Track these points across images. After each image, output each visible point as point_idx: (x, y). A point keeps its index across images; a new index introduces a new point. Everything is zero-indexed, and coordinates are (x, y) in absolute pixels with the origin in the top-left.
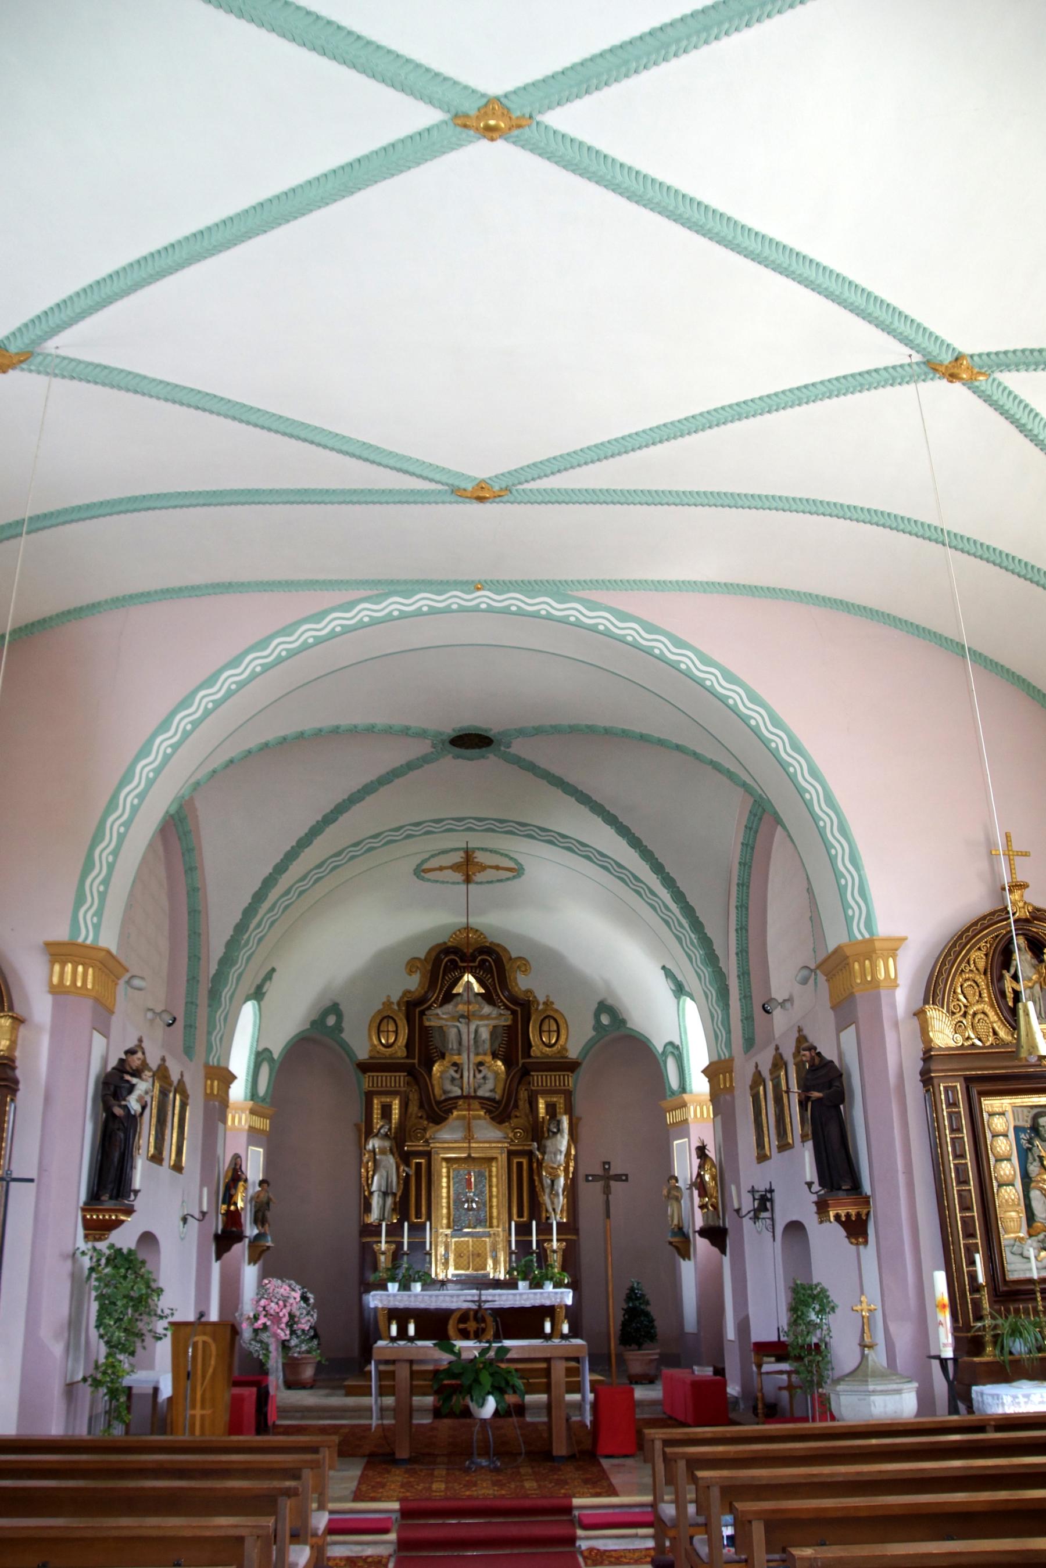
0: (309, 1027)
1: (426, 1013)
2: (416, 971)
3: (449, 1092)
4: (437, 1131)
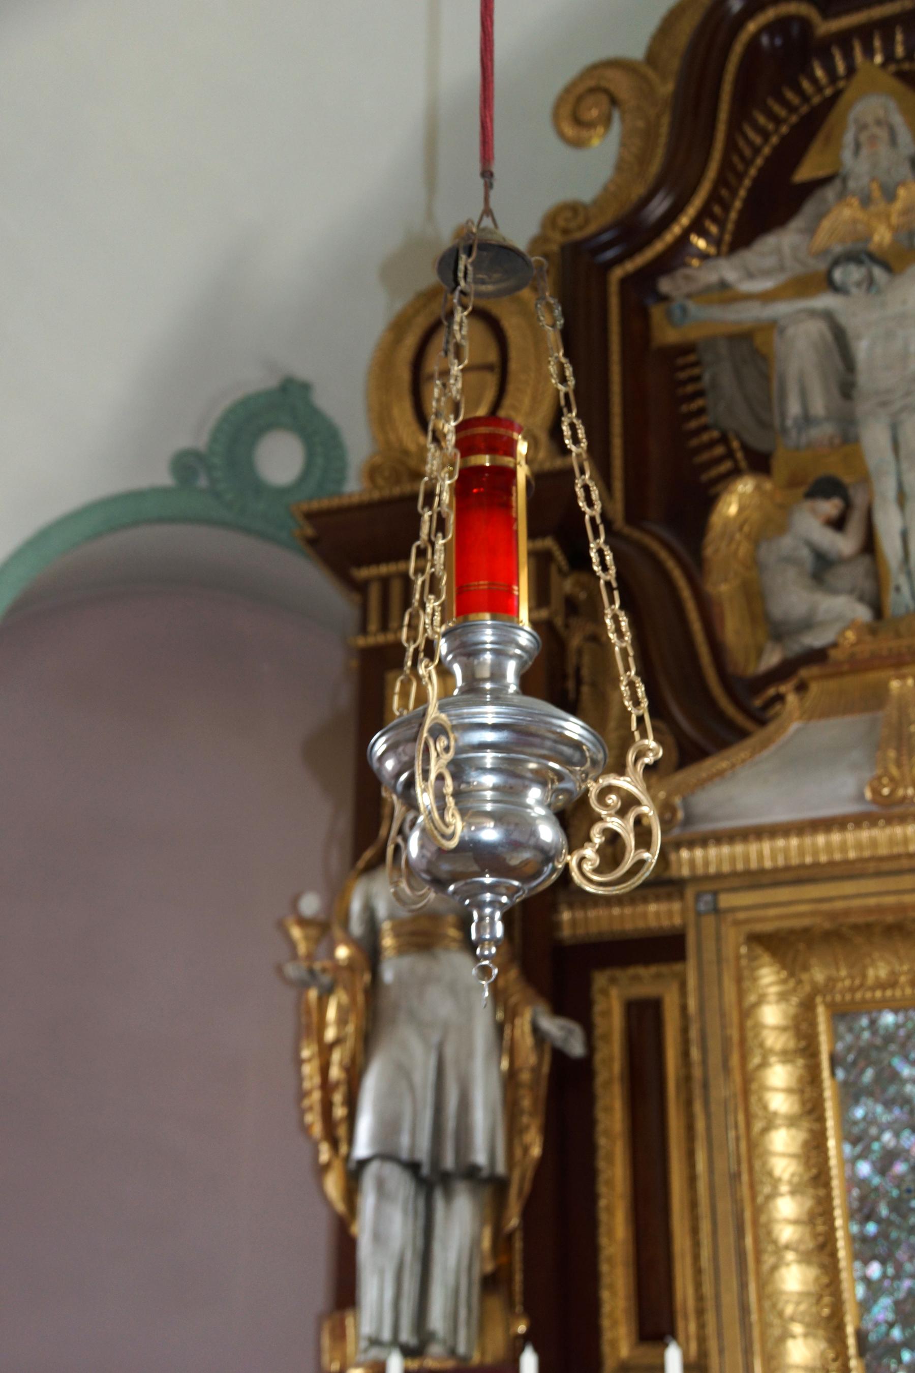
0: (163, 478)
1: (665, 285)
2: (607, 121)
3: (808, 624)
4: (702, 784)
